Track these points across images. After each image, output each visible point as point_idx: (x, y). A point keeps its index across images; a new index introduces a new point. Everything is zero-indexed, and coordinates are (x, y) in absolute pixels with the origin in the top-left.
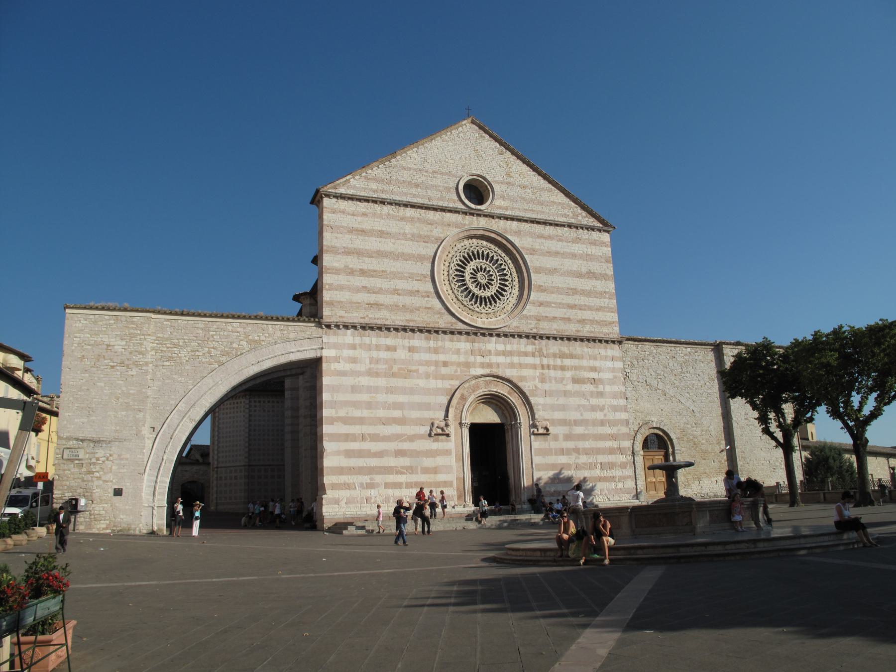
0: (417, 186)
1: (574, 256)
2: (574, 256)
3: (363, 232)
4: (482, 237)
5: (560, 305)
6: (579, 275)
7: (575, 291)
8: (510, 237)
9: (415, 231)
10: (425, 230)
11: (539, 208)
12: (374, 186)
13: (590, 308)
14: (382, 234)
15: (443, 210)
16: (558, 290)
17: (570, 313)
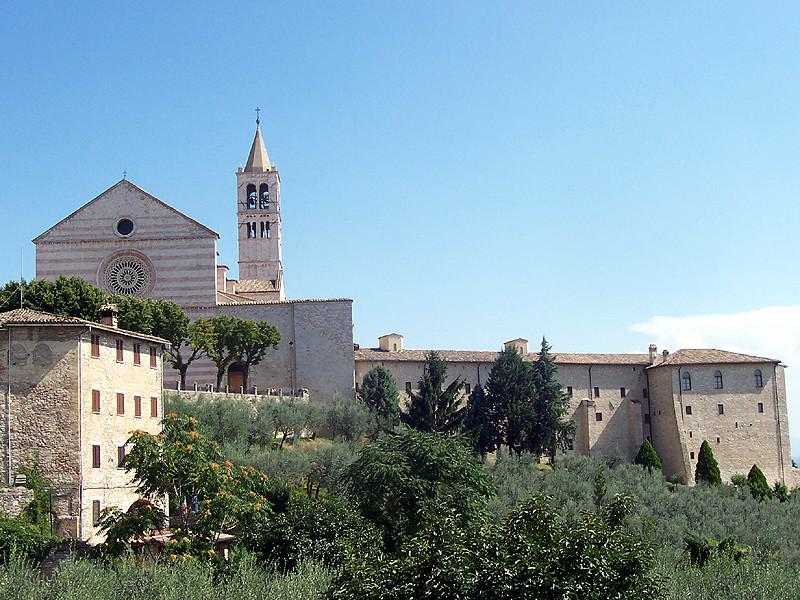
0: (88, 229)
1: (188, 257)
2: (188, 257)
3: (57, 261)
4: (128, 254)
5: (176, 289)
6: (191, 268)
7: (187, 279)
8: (144, 252)
9: (87, 256)
10: (91, 255)
11: (166, 230)
12: (63, 233)
13: (197, 288)
14: (68, 261)
15: (103, 241)
16: (176, 280)
17: (183, 293)
